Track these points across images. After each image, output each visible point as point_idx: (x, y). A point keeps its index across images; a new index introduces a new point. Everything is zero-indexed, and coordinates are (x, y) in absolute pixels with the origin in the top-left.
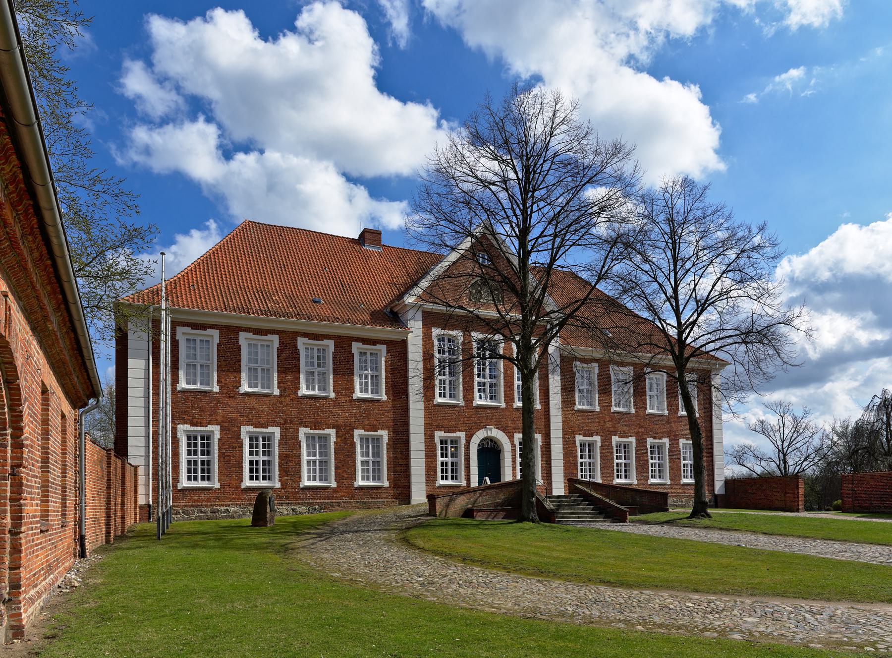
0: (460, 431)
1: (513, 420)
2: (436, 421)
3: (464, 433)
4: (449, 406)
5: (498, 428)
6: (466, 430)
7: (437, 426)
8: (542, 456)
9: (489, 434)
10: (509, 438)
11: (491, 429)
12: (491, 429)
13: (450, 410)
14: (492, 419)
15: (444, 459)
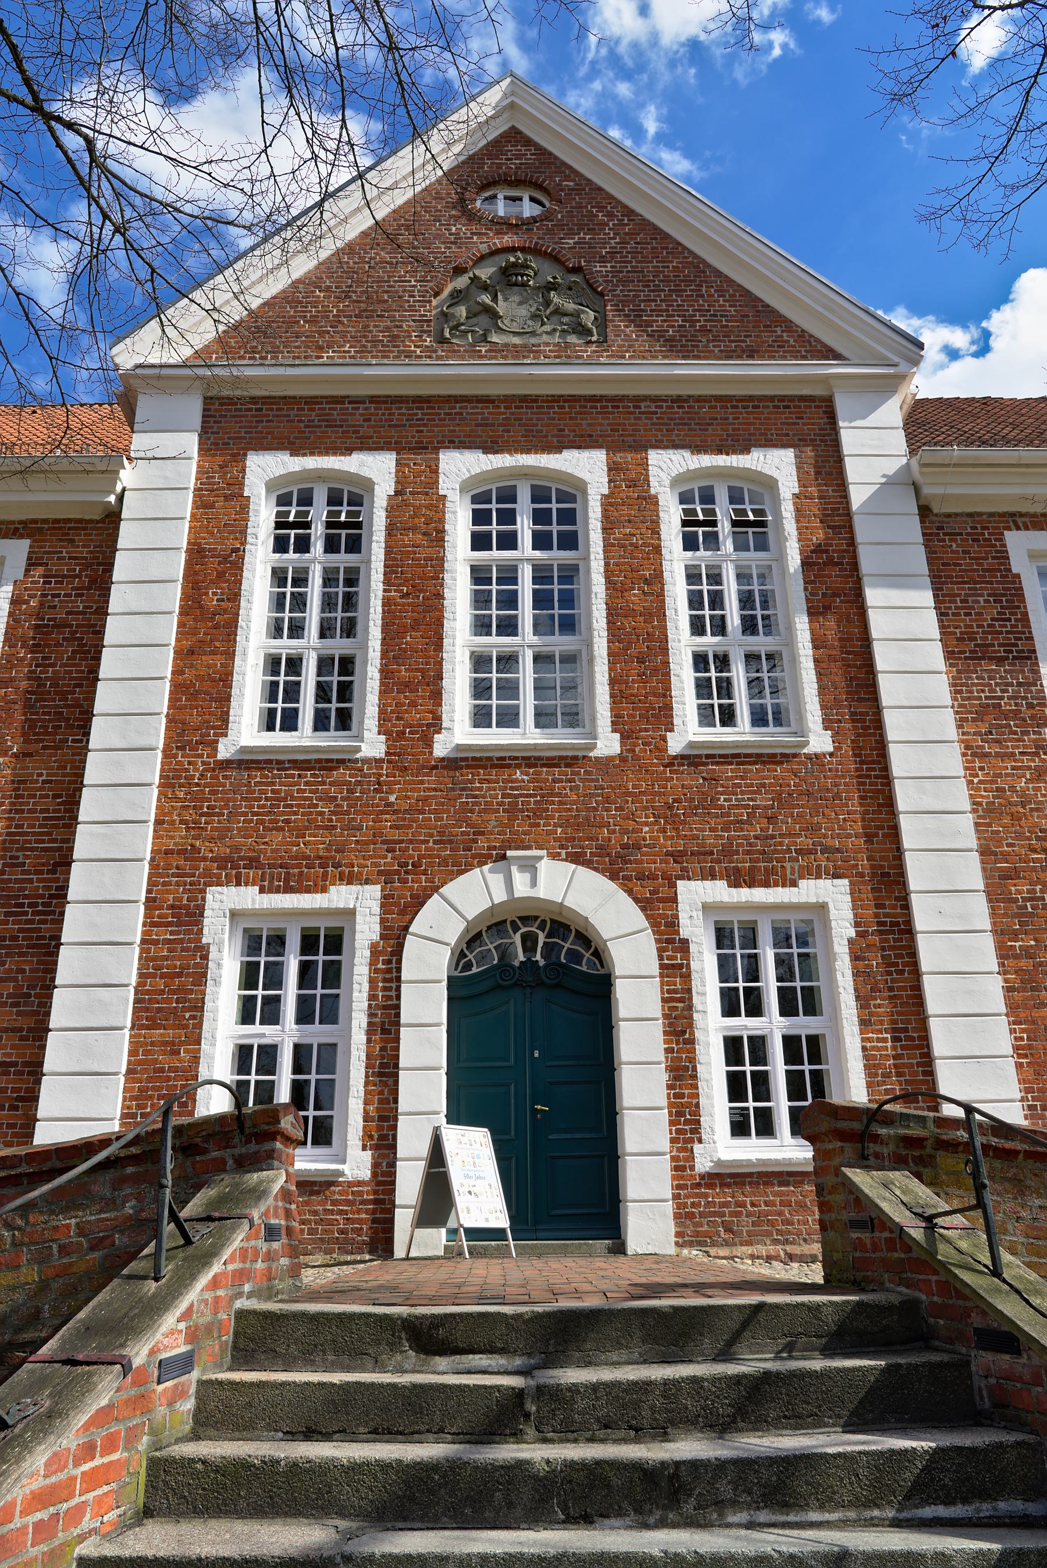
0: (350, 879)
1: (668, 816)
2: (223, 833)
3: (374, 891)
4: (296, 764)
5: (576, 859)
6: (386, 877)
7: (222, 862)
8: (863, 1000)
9: (522, 886)
10: (645, 904)
11: (530, 867)
12: (530, 867)
13: (303, 784)
14: (539, 812)
15: (257, 1028)
